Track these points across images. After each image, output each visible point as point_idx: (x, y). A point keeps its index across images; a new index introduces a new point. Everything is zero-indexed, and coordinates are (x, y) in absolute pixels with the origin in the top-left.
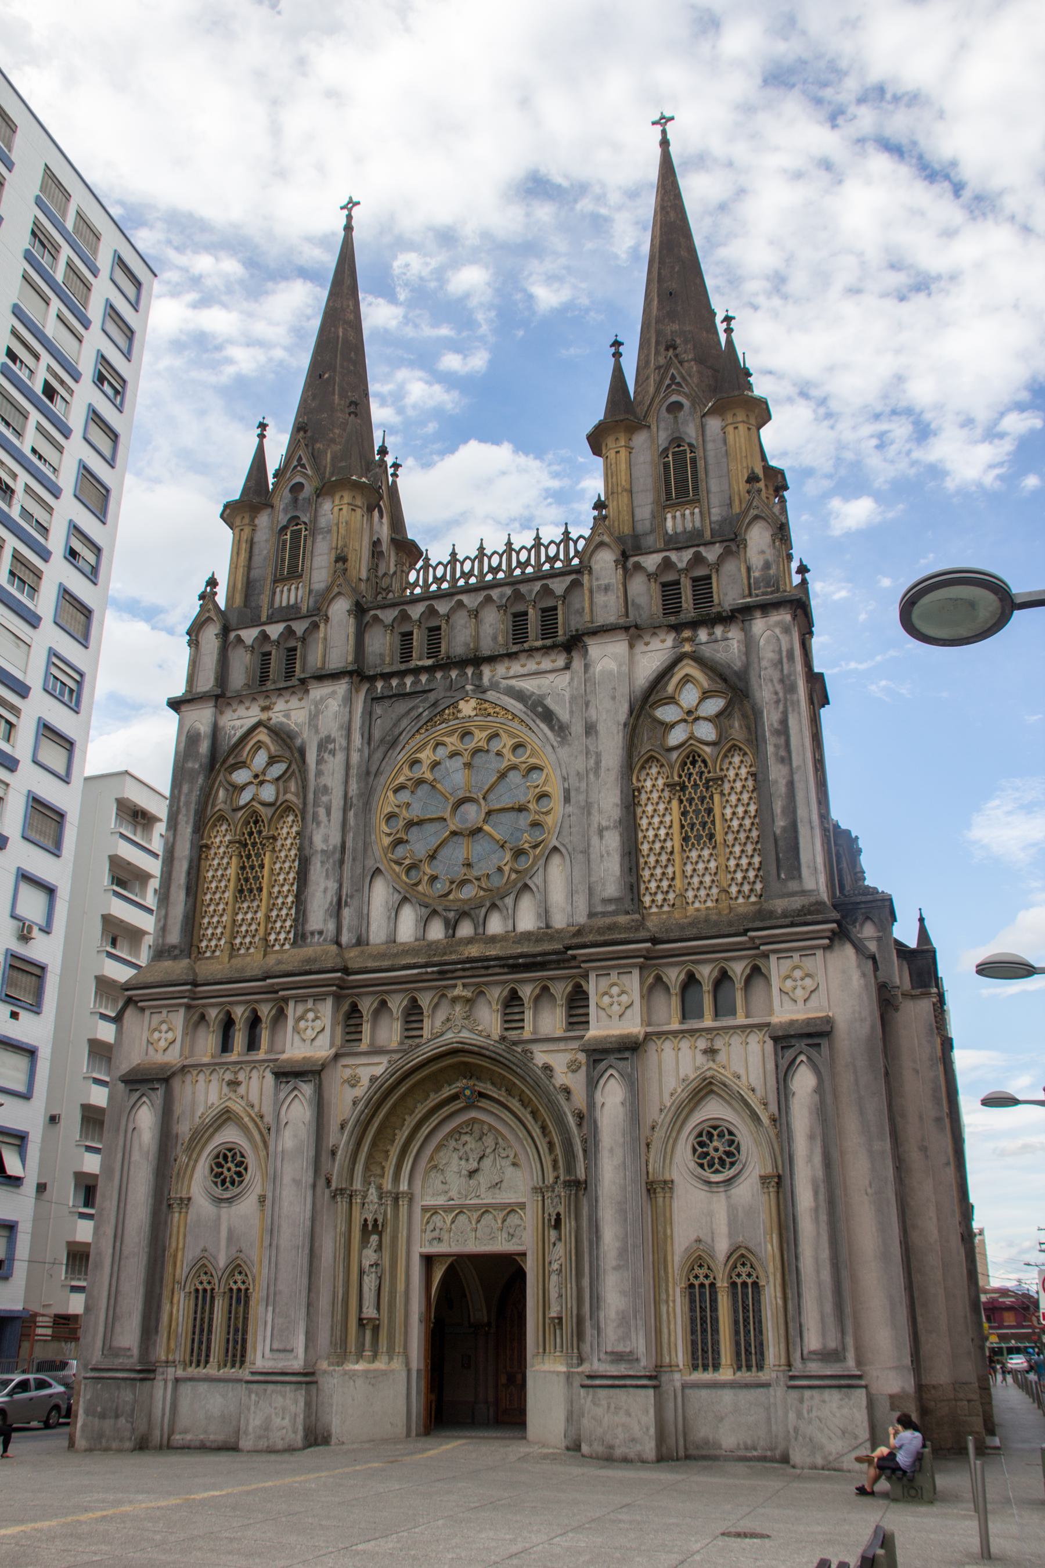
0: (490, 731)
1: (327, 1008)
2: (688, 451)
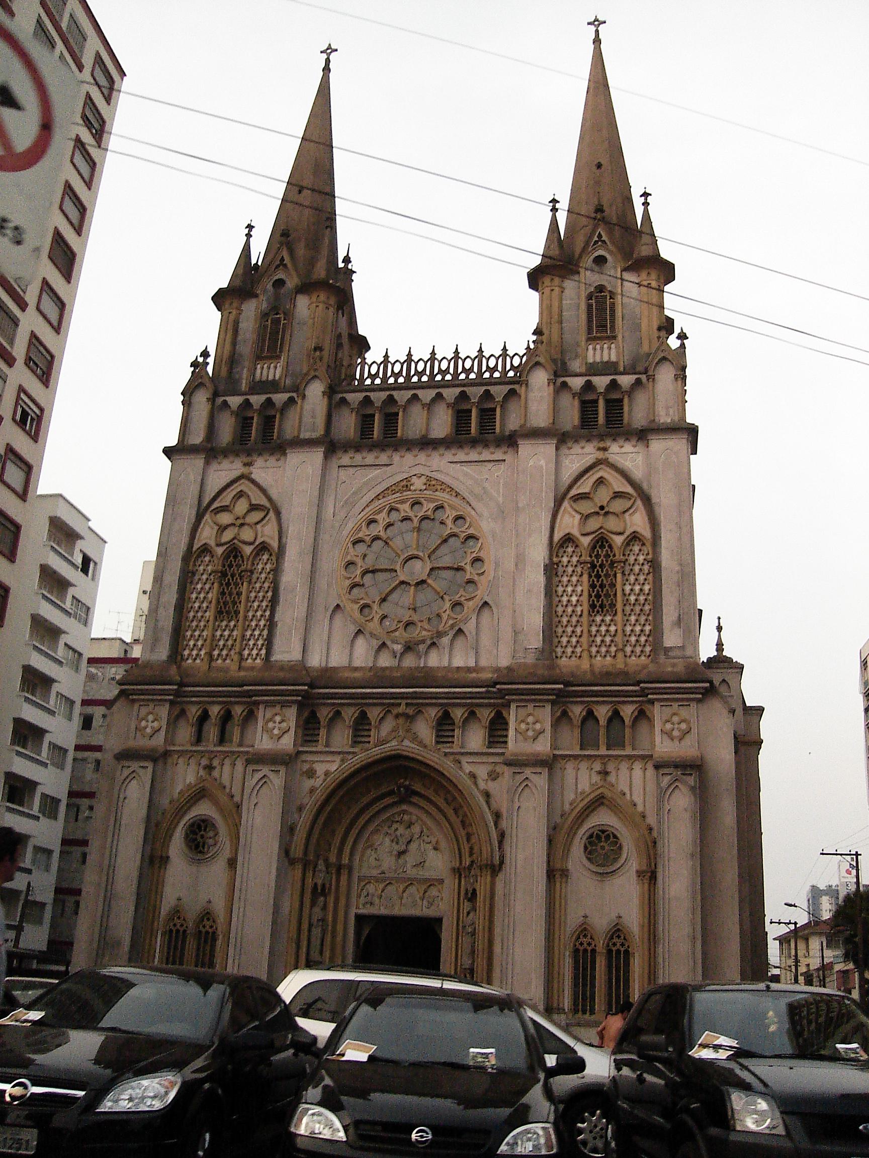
1: (292, 713)
2: (608, 298)
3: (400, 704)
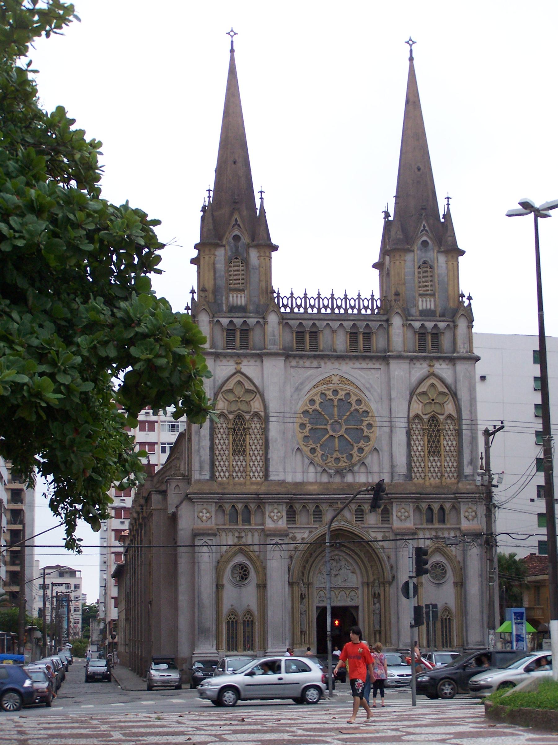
0: (346, 392)
3: (337, 503)
